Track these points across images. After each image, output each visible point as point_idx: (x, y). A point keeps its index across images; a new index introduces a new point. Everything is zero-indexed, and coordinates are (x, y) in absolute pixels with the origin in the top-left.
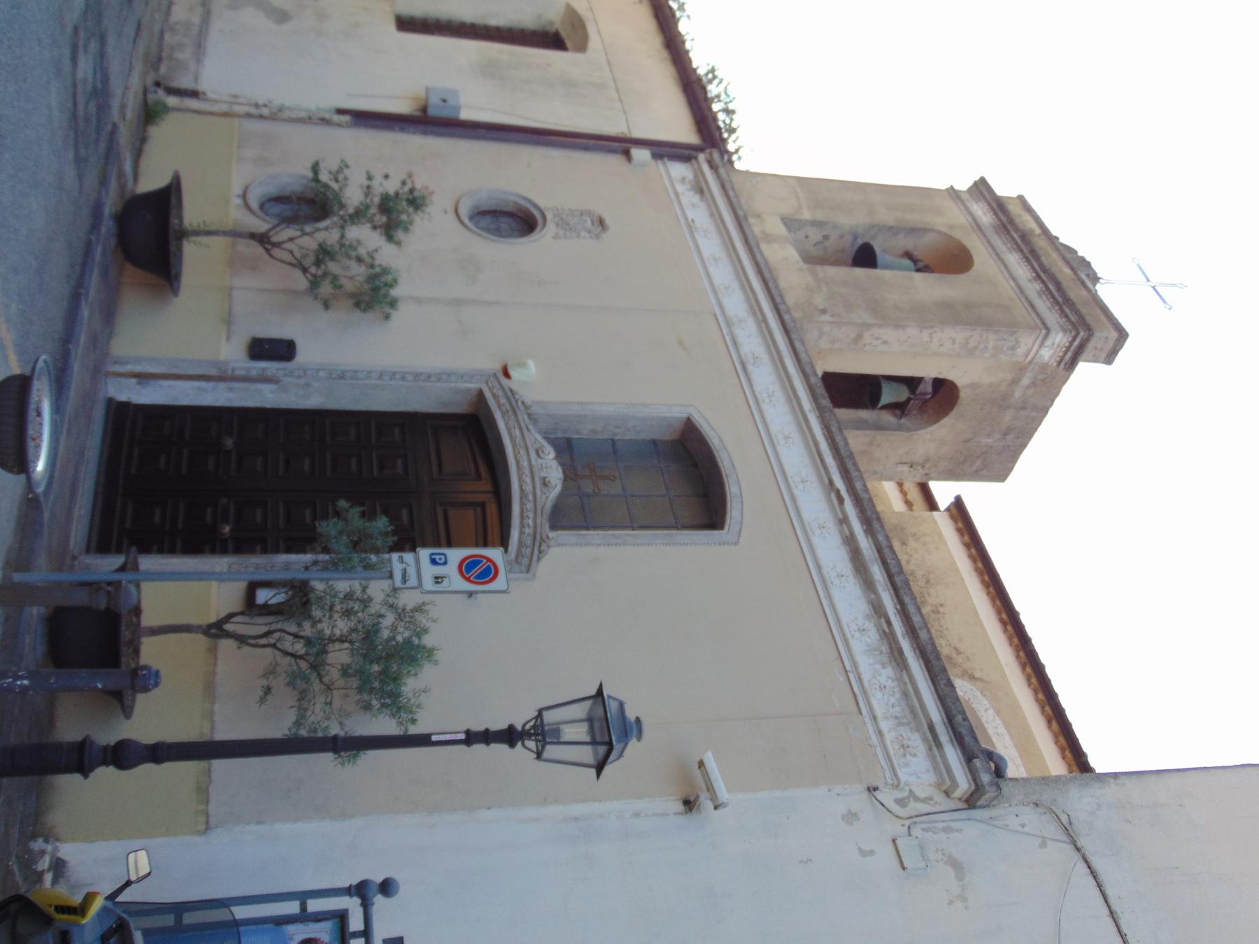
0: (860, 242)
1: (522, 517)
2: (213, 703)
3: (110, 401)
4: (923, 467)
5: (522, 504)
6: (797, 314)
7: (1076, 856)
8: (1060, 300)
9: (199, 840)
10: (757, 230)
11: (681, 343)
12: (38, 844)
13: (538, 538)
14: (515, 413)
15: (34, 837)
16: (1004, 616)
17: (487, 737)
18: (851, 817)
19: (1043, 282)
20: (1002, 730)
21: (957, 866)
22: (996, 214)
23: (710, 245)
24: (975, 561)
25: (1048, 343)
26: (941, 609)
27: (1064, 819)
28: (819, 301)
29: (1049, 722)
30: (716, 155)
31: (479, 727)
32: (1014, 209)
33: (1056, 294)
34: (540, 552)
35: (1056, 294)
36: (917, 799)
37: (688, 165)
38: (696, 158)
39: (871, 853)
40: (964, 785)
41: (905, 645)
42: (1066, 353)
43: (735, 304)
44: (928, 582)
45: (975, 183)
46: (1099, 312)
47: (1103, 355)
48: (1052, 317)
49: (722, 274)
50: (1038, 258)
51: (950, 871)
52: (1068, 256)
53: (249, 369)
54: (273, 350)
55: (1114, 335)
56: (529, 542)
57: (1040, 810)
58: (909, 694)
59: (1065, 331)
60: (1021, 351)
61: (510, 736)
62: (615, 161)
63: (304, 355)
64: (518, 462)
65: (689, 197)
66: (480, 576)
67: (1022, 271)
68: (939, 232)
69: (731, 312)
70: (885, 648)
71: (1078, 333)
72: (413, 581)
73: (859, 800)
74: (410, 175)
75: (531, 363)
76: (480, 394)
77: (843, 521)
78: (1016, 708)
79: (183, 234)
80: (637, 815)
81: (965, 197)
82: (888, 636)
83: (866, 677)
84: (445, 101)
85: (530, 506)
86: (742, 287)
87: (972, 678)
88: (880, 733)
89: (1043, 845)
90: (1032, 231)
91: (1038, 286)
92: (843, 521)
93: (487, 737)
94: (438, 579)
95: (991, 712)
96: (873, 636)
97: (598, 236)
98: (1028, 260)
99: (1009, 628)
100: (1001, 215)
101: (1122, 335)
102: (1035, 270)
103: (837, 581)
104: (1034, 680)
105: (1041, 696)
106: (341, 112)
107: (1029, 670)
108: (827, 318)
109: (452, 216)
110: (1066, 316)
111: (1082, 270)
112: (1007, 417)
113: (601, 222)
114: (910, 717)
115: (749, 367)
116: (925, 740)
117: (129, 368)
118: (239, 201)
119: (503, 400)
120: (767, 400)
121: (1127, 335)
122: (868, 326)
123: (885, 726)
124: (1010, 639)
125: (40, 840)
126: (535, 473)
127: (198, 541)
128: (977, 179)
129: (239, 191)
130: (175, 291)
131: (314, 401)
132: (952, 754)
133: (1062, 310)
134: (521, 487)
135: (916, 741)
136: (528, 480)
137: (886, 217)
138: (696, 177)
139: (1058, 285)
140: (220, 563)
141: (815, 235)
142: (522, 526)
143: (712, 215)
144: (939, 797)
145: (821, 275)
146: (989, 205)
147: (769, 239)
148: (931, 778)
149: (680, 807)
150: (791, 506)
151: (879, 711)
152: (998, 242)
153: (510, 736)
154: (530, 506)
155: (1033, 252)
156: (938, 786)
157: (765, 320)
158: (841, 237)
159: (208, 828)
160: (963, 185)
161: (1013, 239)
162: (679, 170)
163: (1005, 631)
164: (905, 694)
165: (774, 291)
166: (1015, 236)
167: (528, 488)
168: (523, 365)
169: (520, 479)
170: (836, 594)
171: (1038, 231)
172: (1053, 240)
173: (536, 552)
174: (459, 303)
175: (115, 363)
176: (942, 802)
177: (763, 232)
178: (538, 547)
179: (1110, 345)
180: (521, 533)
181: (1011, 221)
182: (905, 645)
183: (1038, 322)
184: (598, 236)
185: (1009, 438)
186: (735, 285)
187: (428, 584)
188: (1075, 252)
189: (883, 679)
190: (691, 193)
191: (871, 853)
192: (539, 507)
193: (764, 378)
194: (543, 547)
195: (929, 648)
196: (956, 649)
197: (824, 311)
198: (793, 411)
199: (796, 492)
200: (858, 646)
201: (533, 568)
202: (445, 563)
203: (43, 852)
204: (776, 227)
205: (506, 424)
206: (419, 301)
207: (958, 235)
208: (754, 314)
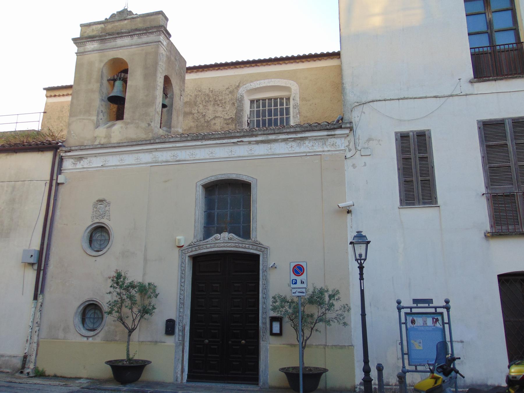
0: (106, 99)
1: (246, 248)
2: (312, 345)
3: (187, 381)
4: (181, 91)
5: (240, 247)
6: (151, 135)
7: (368, 104)
8: (145, 32)
9: (355, 348)
10: (103, 141)
11: (166, 181)
12: (357, 390)
15: (355, 391)
16: (217, 68)
17: (361, 274)
18: (354, 166)
19: (134, 35)
20: (258, 82)
21: (369, 140)
22: (94, 41)
23: (113, 161)
24: (193, 72)
25: (162, 41)
26: (211, 89)
27: (357, 104)
28: (144, 125)
29: (257, 66)
30: (64, 149)
31: (358, 276)
32: (89, 32)
33: (141, 32)
35: (141, 32)
36: (349, 145)
37: (64, 160)
38: (62, 156)
39: (365, 163)
40: (347, 131)
41: (299, 135)
42: (166, 36)
43: (146, 158)
44: (199, 91)
45: (75, 43)
46: (149, 17)
47: (166, 21)
48: (152, 38)
49: (129, 159)
50: (122, 33)
51: (371, 142)
52: (117, 18)
54: (170, 327)
55: (161, 16)
56: (255, 247)
57: (353, 110)
58: (316, 139)
59: (160, 35)
60: (164, 53)
61: (361, 268)
62: (61, 189)
63: (173, 317)
64: (221, 247)
65: (84, 163)
66: (301, 269)
67: (126, 41)
68: (104, 66)
69: (150, 160)
70: (299, 141)
71: (162, 31)
72: (304, 290)
73: (349, 162)
74: (110, 278)
75: (178, 238)
76: (189, 256)
77: (250, 143)
78: (251, 75)
79: (129, 360)
80: (351, 227)
81: (82, 49)
82: (295, 139)
83: (308, 150)
84: (32, 256)
85: (240, 245)
86: (137, 153)
87: (238, 86)
88: (329, 151)
89: (364, 113)
90: (102, 28)
91: (136, 38)
92: (250, 143)
93: (361, 274)
94: (302, 282)
95: (252, 84)
96: (294, 144)
97: (109, 204)
98: (122, 37)
99: (221, 68)
100: (97, 39)
101: (161, 13)
102: (128, 36)
103: (273, 150)
104: (242, 66)
105: (248, 66)
106: (36, 298)
107: (238, 67)
108: (152, 124)
109: (98, 259)
110: (153, 32)
111: (124, 15)
112: (173, 58)
113: (101, 201)
114: (323, 140)
115: (178, 159)
116: (331, 138)
117: (179, 376)
118: (90, 339)
119: (194, 249)
120: (194, 156)
121: (162, 11)
122: (156, 109)
123: (326, 149)
124: (225, 69)
125: (356, 389)
126: (225, 241)
127: (253, 352)
128: (72, 42)
129: (85, 339)
130: (149, 362)
131: (188, 312)
132: (338, 132)
133: (149, 33)
135: (331, 140)
136: (230, 244)
137: (95, 86)
138: (72, 159)
139: (136, 30)
140: (262, 344)
141: (101, 116)
142: (249, 248)
143: (95, 156)
144: (348, 139)
145: (129, 121)
146: (88, 41)
147: (108, 136)
148: (343, 139)
149: (349, 215)
150: (240, 158)
151: (321, 149)
152: (110, 44)
153: (361, 268)
154: (240, 245)
155: (118, 33)
156: (345, 138)
157: (156, 149)
158: (102, 105)
159: (352, 346)
160: (75, 48)
161: (108, 39)
162: (68, 164)
163: (222, 70)
164: (315, 139)
165: (144, 142)
166: (108, 37)
167: (233, 245)
168: (179, 240)
170: (277, 152)
171: (102, 26)
172: (106, 22)
174: (146, 260)
175: (177, 380)
176: (351, 137)
177: (105, 138)
178: (257, 244)
179: (164, 18)
181: (100, 36)
182: (299, 135)
183: (155, 44)
184: (109, 204)
185: (177, 59)
186: (136, 155)
187: (304, 286)
188: (114, 14)
189: (310, 145)
190: (82, 162)
191: (365, 163)
193: (183, 155)
195: (303, 129)
196: (227, 89)
197: (149, 125)
198: (199, 148)
199: (236, 155)
200: (297, 150)
202: (296, 280)
203: (360, 388)
204: (102, 131)
206: (144, 274)
207: (106, 60)
208: (151, 151)
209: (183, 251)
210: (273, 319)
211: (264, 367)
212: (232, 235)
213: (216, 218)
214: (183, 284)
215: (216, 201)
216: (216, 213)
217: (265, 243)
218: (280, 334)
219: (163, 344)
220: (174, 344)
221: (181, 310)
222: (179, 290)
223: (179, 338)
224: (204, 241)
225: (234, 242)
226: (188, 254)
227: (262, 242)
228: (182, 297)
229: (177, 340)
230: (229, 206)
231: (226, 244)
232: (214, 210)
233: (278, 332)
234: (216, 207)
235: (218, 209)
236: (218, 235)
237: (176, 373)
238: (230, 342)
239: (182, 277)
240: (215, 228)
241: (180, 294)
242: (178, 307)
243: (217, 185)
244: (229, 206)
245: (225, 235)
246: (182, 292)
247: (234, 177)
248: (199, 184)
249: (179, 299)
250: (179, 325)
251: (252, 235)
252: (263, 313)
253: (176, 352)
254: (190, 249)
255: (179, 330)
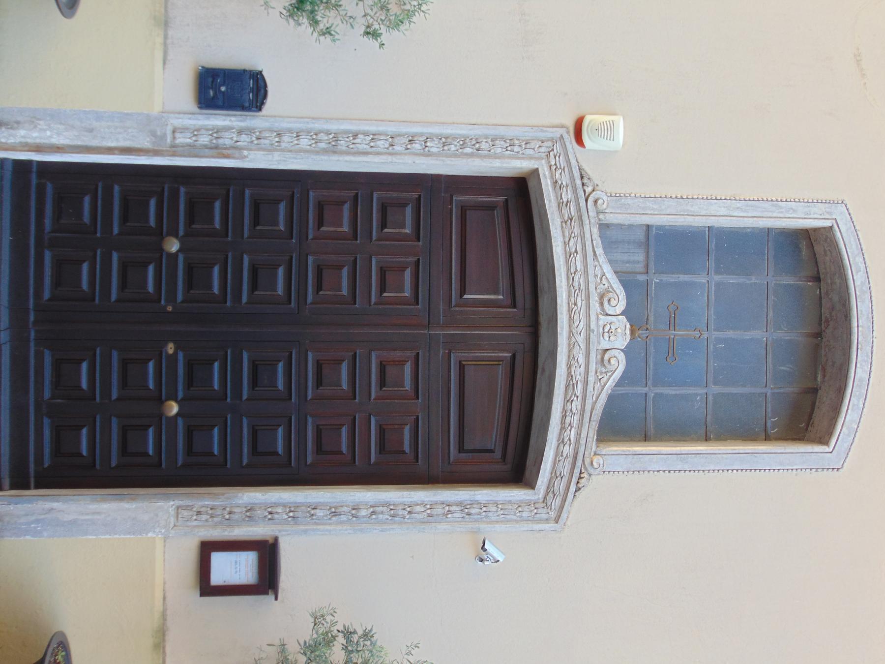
1: (563, 429)
5: (567, 401)
13: (579, 463)
14: (582, 225)
34: (578, 489)
53: (196, 132)
54: (230, 89)
56: (566, 472)
64: (571, 319)
85: (576, 404)
126: (592, 333)
134: (569, 368)
136: (582, 360)
142: (561, 441)
154: (576, 404)
167: (578, 374)
168: (608, 131)
169: (570, 357)
173: (573, 488)
178: (578, 474)
180: (558, 453)
192: (588, 408)
194: (582, 481)
201: (564, 515)
205: (566, 244)
209: (558, 148)
210: (268, 554)
211: (68, 518)
212: (619, 364)
213: (683, 278)
214: (417, 146)
215: (754, 280)
216: (702, 279)
217: (578, 508)
218: (207, 588)
219: (159, 55)
220: (157, 109)
221: (305, 142)
222: (391, 129)
223: (184, 129)
224: (595, 230)
225: (591, 379)
226: (544, 172)
227: (581, 494)
228: (362, 143)
229: (178, 122)
230: (730, 334)
231: (581, 339)
232: (718, 272)
233: (217, 578)
234: (732, 280)
235: (718, 285)
236: (622, 306)
237: (34, 118)
238: (170, 348)
239: (445, 140)
240: (642, 278)
241: (375, 137)
242: (318, 126)
243: (817, 279)
244: (730, 334)
245: (618, 335)
246: (382, 144)
247: (858, 371)
248: (839, 214)
249: (353, 127)
250: (240, 132)
251: (619, 453)
252: (292, 508)
253: (128, 115)
254: (565, 180)
255: (218, 130)
